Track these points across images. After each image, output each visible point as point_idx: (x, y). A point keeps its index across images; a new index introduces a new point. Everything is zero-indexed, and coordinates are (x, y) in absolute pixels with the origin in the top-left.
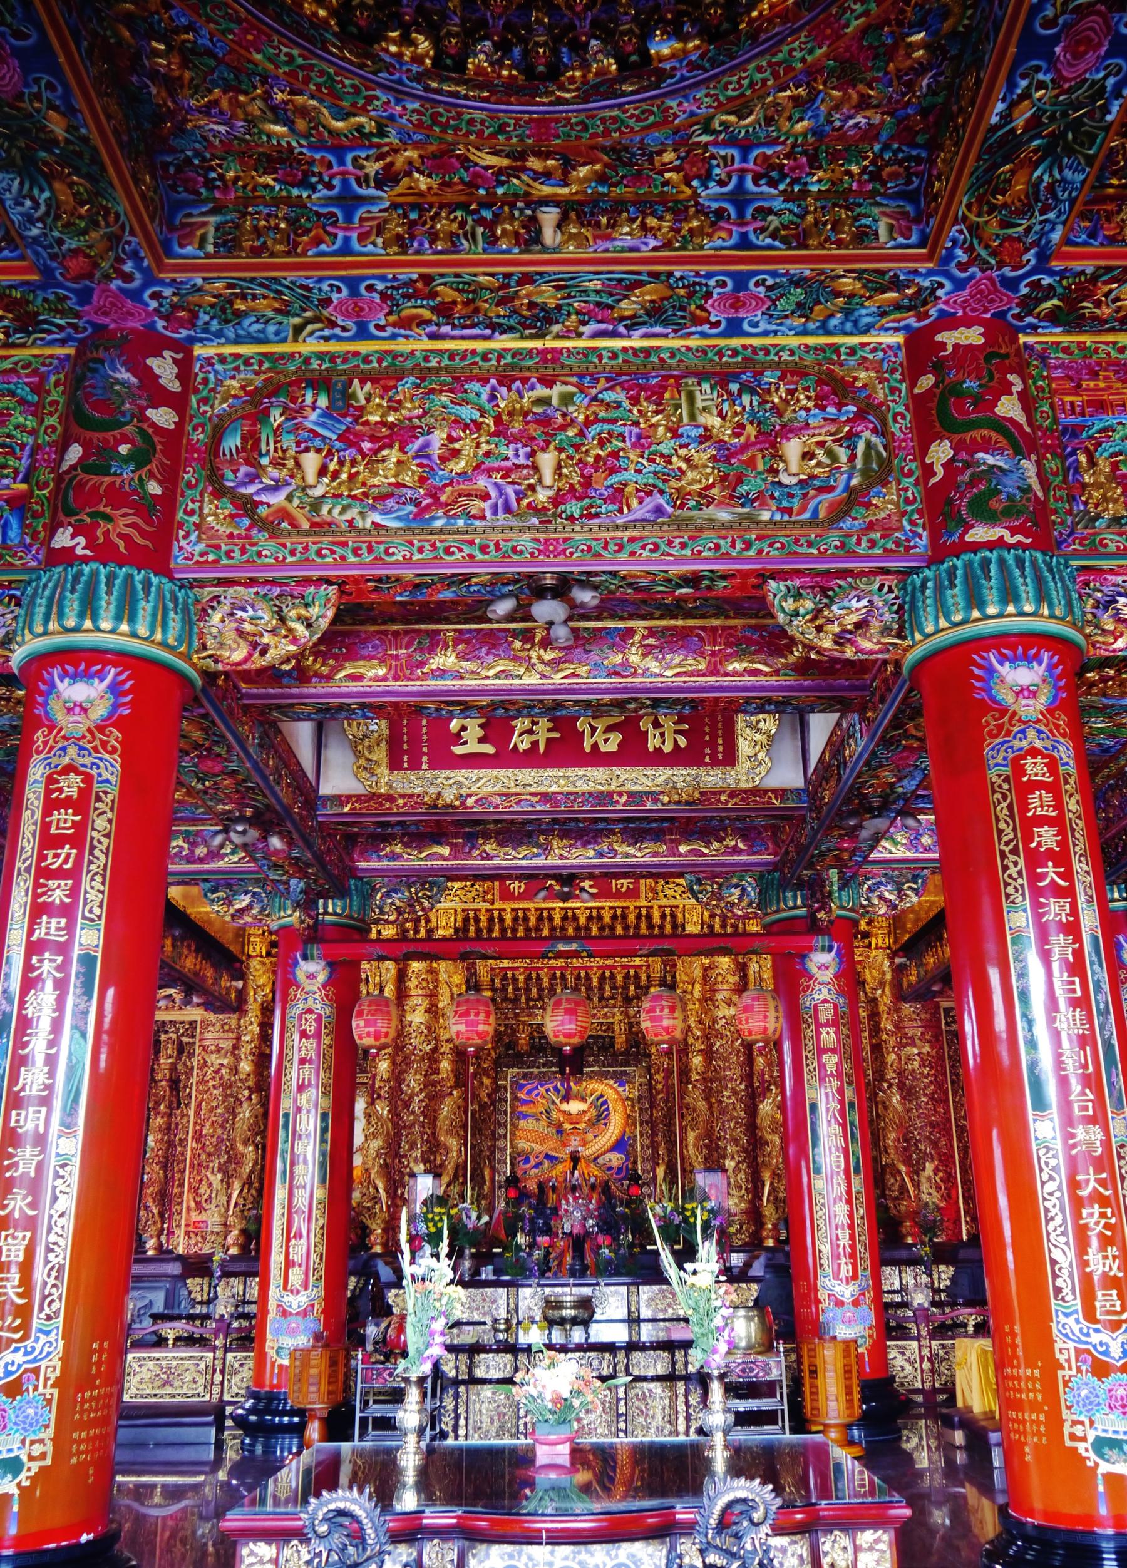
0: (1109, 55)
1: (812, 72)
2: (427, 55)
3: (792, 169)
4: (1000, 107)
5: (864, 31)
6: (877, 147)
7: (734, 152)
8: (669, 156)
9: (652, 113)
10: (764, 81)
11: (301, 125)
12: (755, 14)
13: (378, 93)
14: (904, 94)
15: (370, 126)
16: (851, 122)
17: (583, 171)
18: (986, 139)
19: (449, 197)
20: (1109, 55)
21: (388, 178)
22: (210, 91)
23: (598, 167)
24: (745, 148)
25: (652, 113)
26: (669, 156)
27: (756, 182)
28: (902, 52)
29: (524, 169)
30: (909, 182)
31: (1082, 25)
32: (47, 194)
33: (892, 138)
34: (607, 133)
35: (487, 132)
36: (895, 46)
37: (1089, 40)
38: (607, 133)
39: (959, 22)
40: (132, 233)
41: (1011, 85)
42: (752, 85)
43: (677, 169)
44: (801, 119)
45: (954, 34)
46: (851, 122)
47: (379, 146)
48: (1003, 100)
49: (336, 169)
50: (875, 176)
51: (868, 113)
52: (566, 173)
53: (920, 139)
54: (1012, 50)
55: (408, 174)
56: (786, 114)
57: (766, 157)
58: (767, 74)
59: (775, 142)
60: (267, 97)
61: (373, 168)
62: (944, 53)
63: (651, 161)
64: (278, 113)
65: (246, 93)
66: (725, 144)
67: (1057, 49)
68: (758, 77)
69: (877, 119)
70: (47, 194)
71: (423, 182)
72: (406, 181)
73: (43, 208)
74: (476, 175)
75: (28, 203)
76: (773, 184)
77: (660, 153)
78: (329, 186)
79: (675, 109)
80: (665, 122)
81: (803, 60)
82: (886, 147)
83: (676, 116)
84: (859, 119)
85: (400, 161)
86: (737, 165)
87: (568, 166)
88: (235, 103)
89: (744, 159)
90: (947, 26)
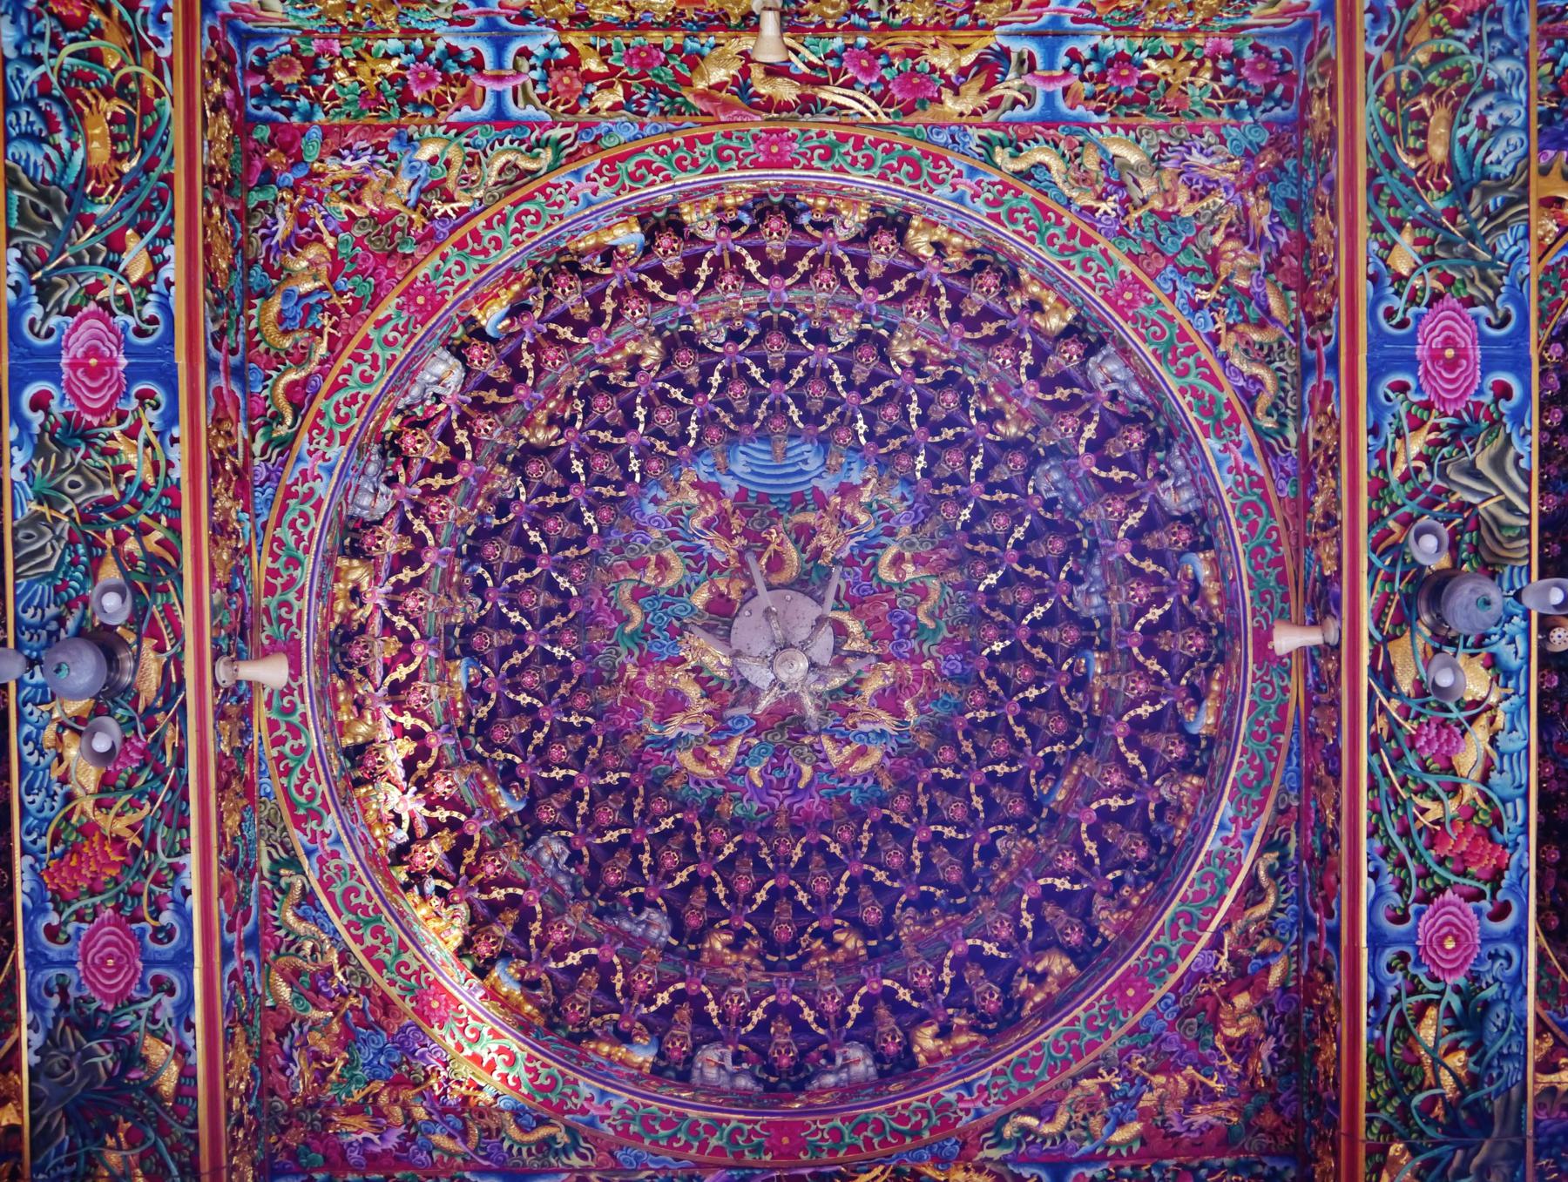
0: (55, 351)
1: (429, 239)
2: (918, 230)
3: (431, 78)
4: (167, 272)
5: (376, 300)
6: (320, 117)
7: (515, 111)
8: (605, 100)
9: (632, 176)
10: (489, 226)
11: (1091, 161)
12: (516, 287)
13: (986, 210)
14: (304, 204)
15: (1001, 156)
16: (365, 160)
17: (718, 75)
18: (172, 215)
19: (909, 39)
20: (55, 351)
21: (991, 66)
22: (1196, 215)
23: (701, 85)
24: (500, 119)
25: (632, 176)
26: (605, 100)
27: (478, 63)
28: (323, 269)
29: (802, 79)
30: (261, 53)
31: (107, 394)
32: (1461, 132)
33: (303, 131)
34: (690, 143)
35: (849, 147)
36: (332, 279)
37: (93, 373)
38: (690, 143)
39: (264, 311)
40: (1369, 59)
41: (164, 306)
42: (504, 220)
43: (589, 77)
44: (433, 161)
45: (264, 294)
46: (365, 160)
47: (994, 125)
48: (169, 284)
49: (1058, 88)
50: (311, 65)
51: (343, 174)
52: (745, 71)
53: (263, 132)
54: (181, 360)
55: (963, 72)
56: (454, 172)
57: (469, 99)
58: (487, 236)
59: (461, 128)
60: (1126, 204)
61: (1010, 85)
62: (267, 267)
63: (628, 94)
64: (1116, 180)
65: (1152, 211)
66: (531, 125)
67: (123, 362)
68: (499, 232)
69: (332, 164)
70: (1461, 132)
71: (944, 60)
72: (967, 59)
73: (1477, 108)
74: (868, 72)
75: (1492, 119)
76: (453, 52)
77: (616, 107)
78: (1074, 55)
79: (601, 181)
80: (611, 162)
81: (444, 257)
82: (308, 116)
83: (598, 171)
84: (356, 166)
85: (971, 99)
86: (507, 87)
87: (741, 82)
88: (1168, 195)
89: (499, 96)
90: (276, 304)
